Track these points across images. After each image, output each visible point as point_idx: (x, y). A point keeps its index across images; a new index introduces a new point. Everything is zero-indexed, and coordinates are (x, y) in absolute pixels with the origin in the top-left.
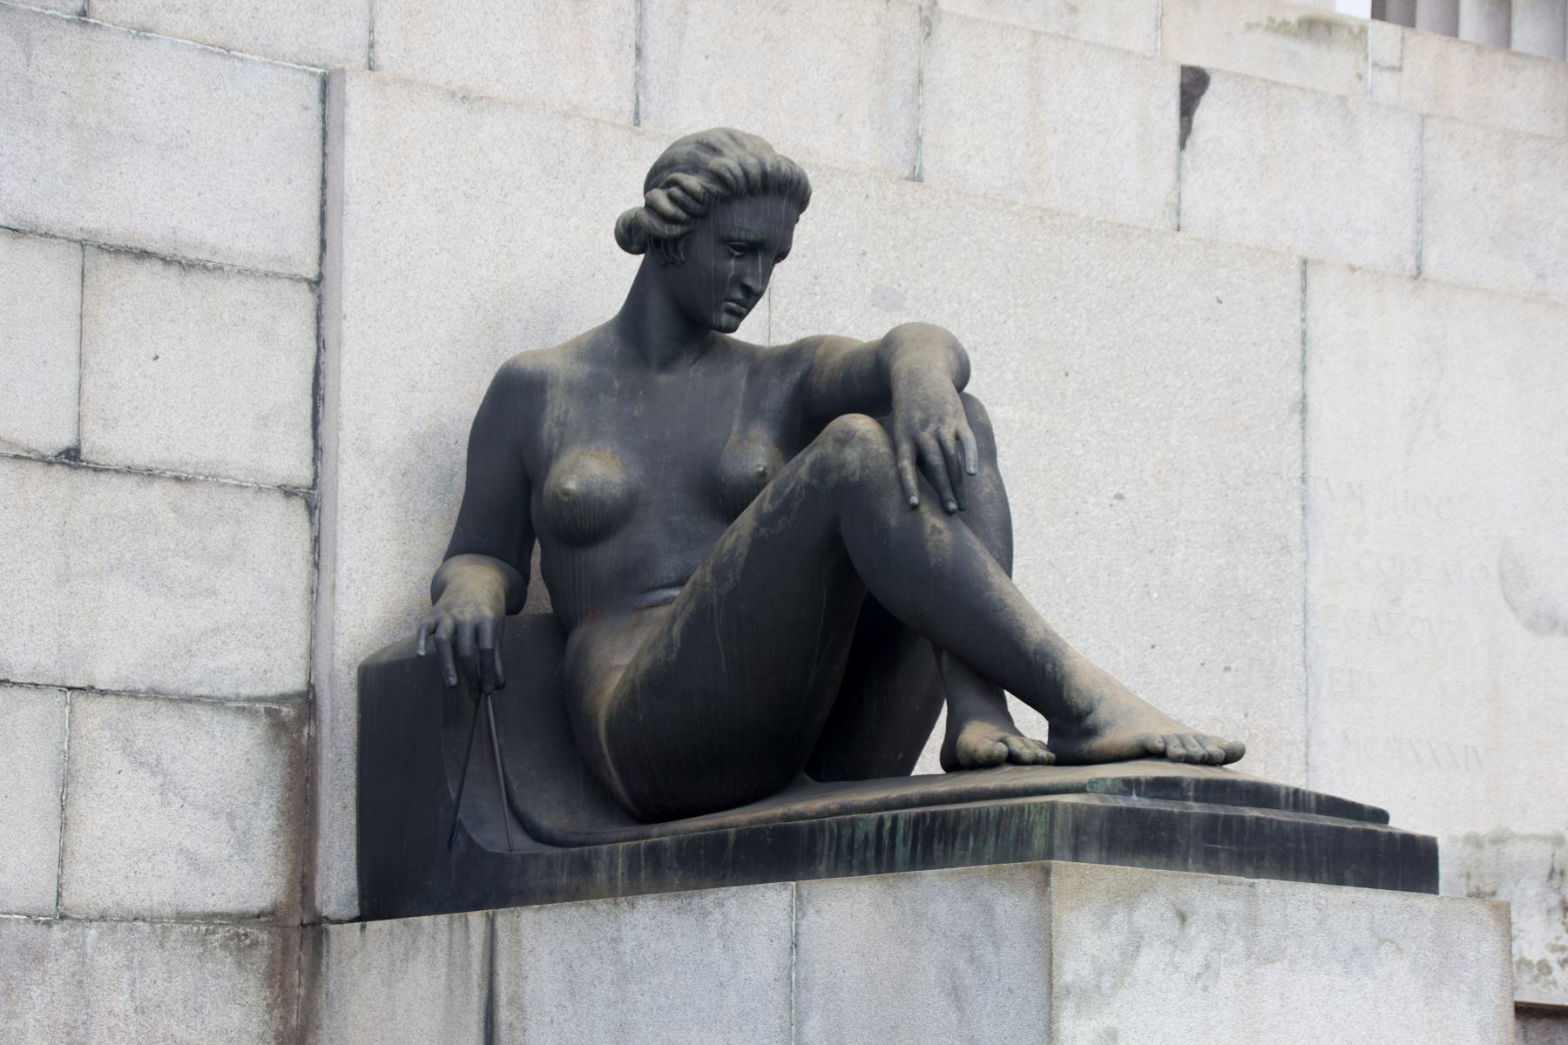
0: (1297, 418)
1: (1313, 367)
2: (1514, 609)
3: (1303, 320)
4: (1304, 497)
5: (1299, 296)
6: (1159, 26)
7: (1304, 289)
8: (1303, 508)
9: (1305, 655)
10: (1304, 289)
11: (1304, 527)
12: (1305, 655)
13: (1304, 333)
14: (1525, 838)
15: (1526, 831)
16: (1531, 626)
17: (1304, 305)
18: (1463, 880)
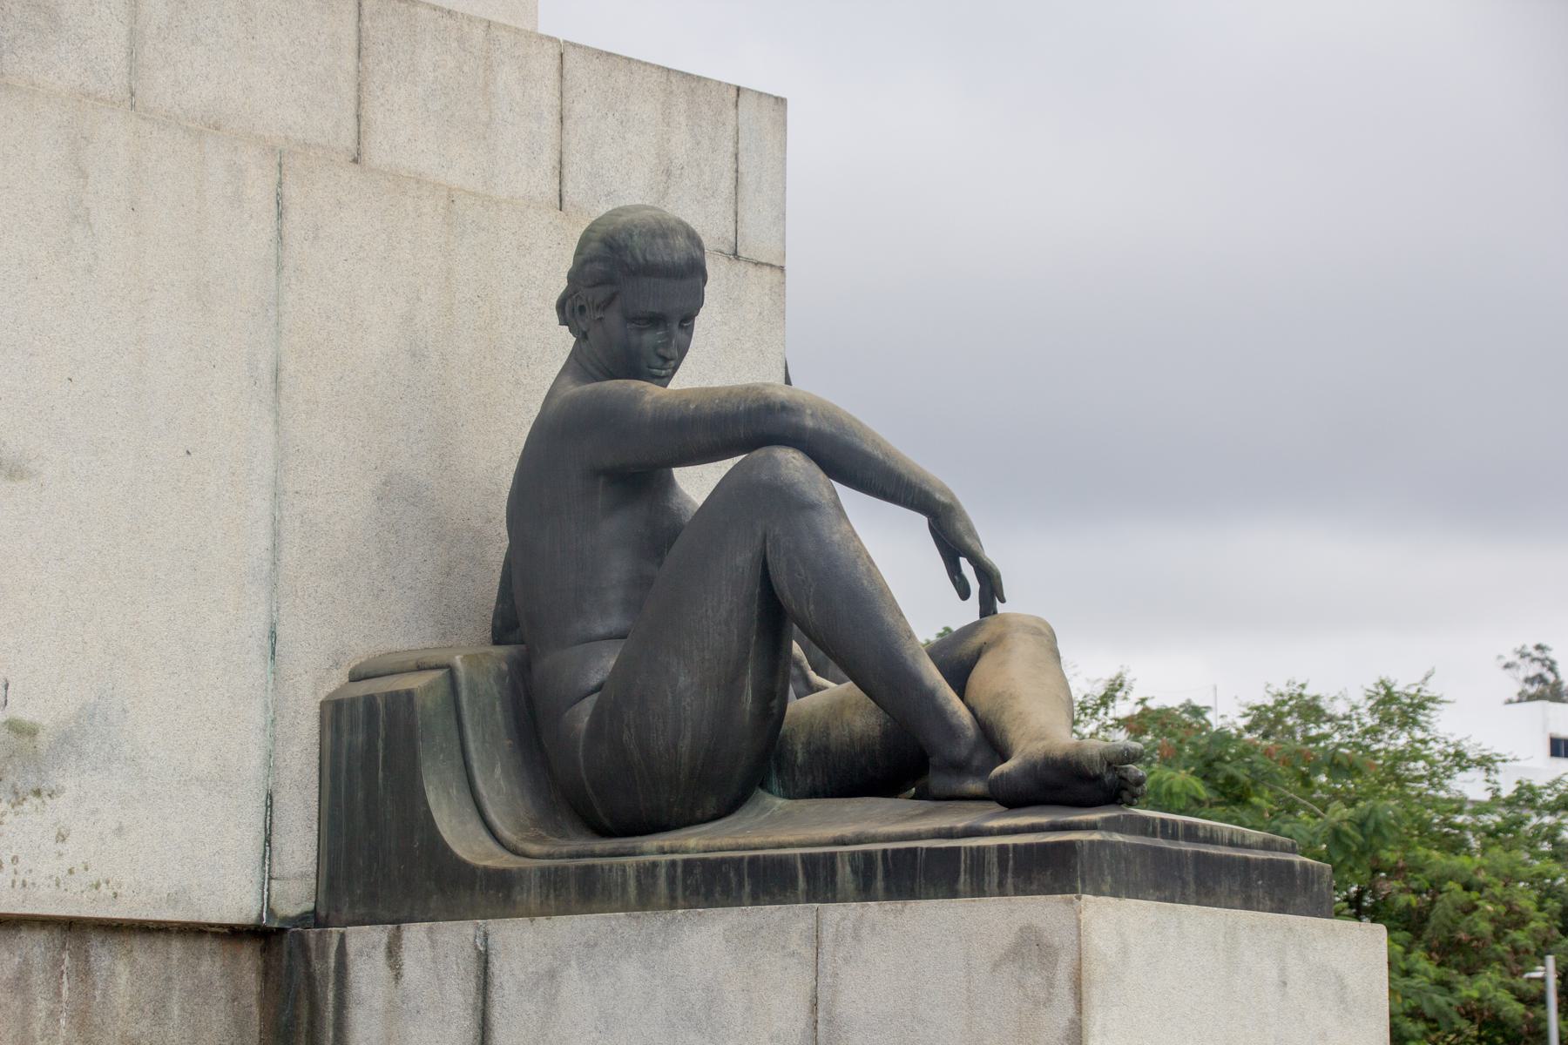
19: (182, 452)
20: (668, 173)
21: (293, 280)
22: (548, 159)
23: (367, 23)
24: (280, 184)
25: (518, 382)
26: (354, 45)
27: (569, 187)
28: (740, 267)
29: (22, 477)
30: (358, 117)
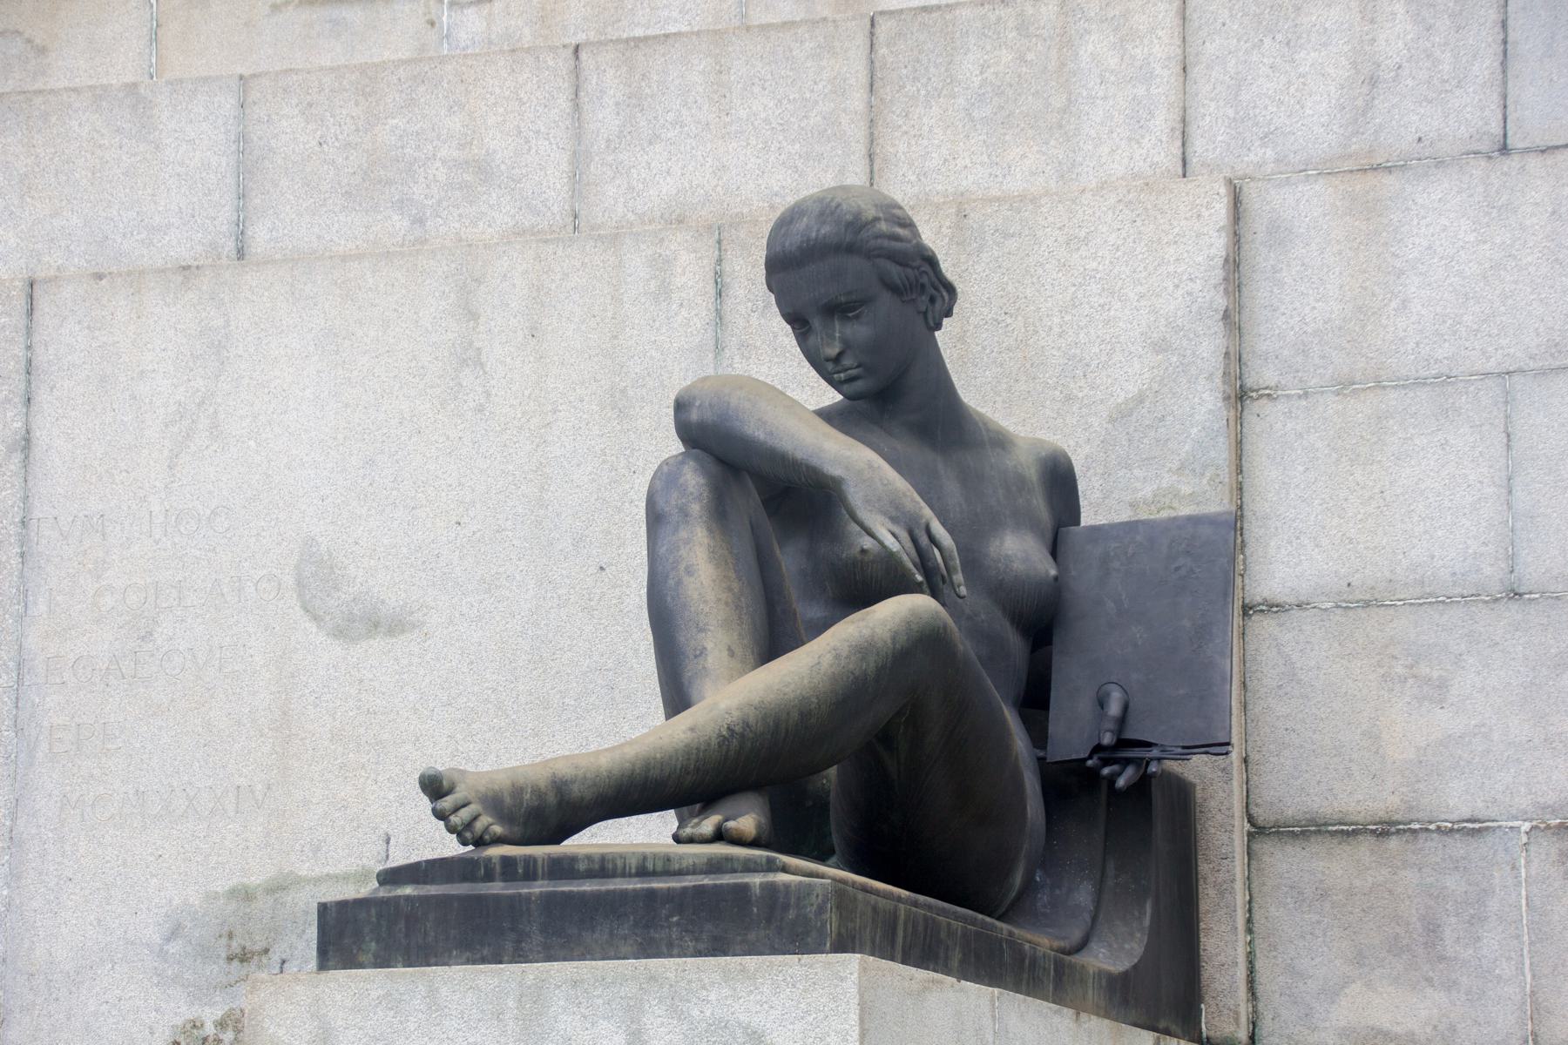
0: (17, 457)
1: (42, 396)
2: (316, 618)
3: (29, 348)
4: (23, 541)
5: (23, 322)
6: (155, 38)
7: (30, 312)
8: (22, 555)
9: (16, 716)
10: (30, 312)
11: (21, 576)
12: (16, 716)
13: (29, 362)
14: (317, 881)
15: (317, 872)
16: (340, 633)
17: (29, 331)
18: (224, 941)
19: (593, 570)
20: (1373, 81)
21: (737, 359)
22: (1162, 121)
23: (882, 51)
24: (720, 261)
25: (1069, 398)
26: (863, 78)
27: (1198, 146)
28: (1514, 162)
29: (403, 631)
30: (871, 157)
